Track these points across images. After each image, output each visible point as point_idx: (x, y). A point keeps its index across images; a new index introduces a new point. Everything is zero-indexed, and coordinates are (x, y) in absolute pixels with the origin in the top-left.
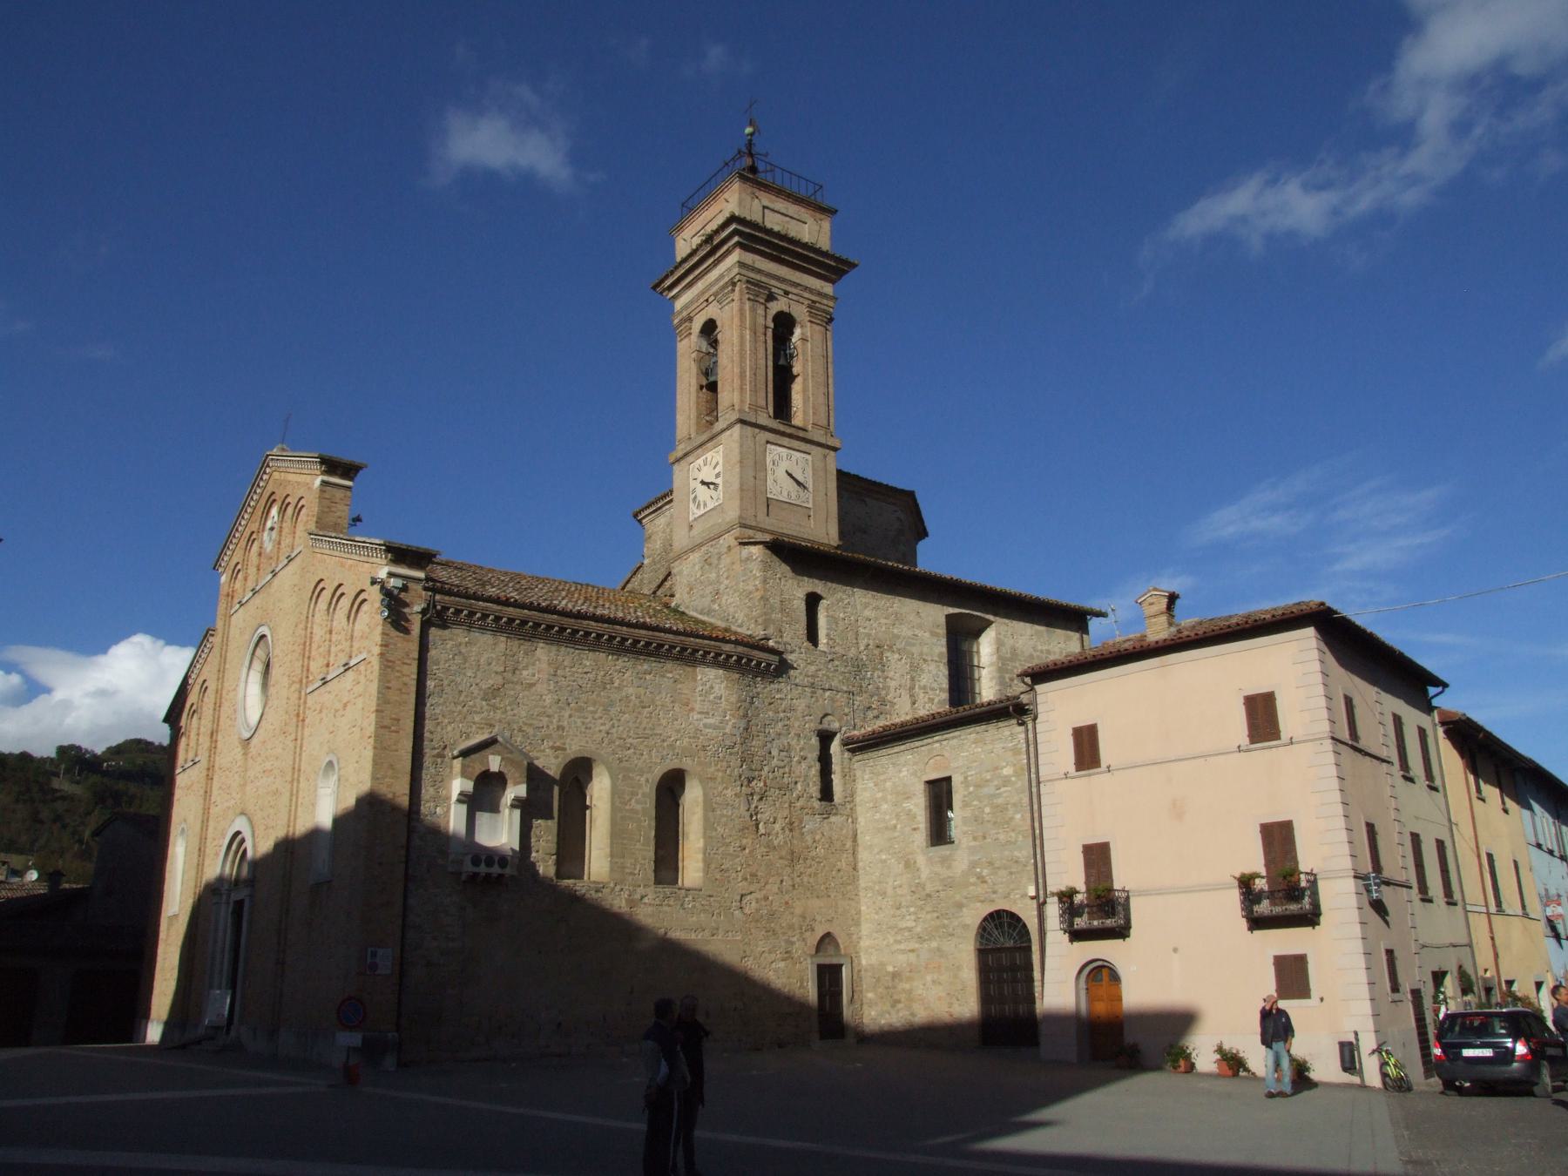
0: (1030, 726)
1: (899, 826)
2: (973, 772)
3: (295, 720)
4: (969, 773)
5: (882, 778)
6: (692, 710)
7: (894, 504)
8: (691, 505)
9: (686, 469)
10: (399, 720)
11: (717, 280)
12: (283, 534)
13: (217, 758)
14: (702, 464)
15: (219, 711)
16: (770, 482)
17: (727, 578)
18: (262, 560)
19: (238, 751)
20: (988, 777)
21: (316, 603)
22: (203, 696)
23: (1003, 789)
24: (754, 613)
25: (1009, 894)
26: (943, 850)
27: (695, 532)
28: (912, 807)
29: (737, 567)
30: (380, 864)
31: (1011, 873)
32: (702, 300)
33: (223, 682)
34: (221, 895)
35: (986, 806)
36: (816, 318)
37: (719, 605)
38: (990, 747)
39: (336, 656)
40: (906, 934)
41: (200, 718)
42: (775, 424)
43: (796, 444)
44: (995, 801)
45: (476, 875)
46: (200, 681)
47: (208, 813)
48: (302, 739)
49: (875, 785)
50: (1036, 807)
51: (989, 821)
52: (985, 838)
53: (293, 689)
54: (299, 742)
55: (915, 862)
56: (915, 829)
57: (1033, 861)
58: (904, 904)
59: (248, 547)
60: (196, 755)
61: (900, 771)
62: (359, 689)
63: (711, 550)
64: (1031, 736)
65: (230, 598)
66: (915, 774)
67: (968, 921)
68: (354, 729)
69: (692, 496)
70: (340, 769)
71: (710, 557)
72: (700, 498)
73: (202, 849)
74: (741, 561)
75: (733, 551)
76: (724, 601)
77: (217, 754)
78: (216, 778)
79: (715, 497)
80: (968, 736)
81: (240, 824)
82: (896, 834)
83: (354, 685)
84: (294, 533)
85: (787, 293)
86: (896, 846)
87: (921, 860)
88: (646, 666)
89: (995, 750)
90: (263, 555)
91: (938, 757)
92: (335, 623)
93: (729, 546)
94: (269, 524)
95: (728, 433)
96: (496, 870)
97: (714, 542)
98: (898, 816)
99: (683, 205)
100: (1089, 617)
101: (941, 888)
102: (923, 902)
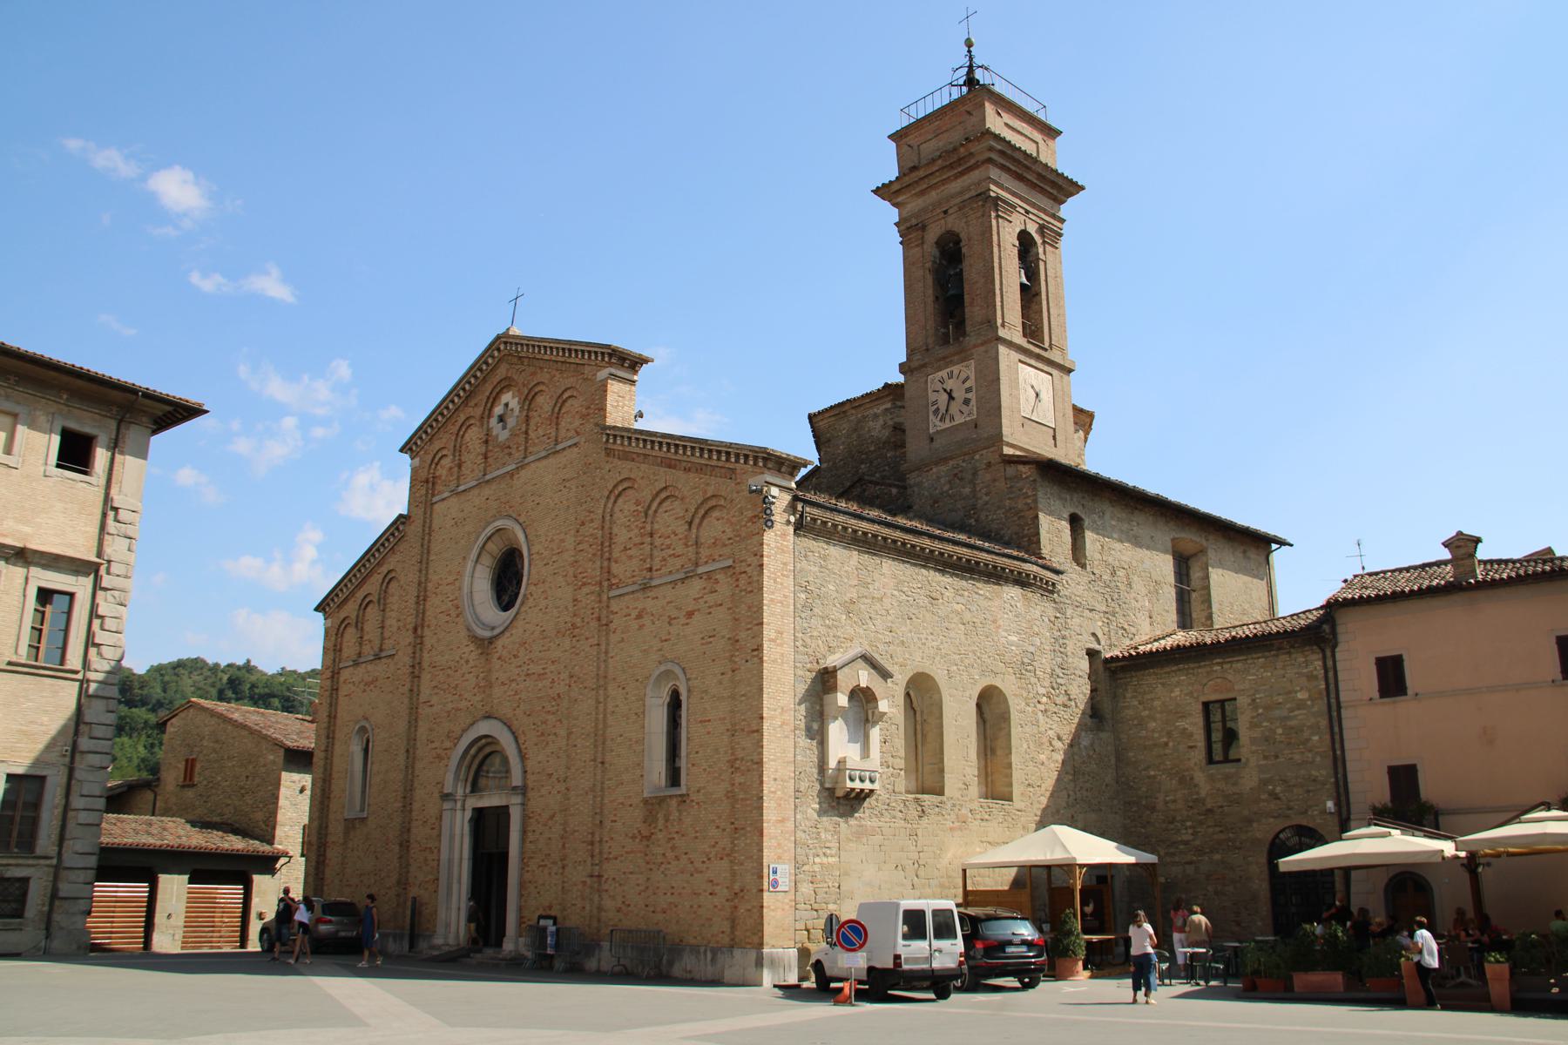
0: (1328, 653)
1: (1171, 744)
2: (1262, 695)
3: (594, 624)
4: (1257, 696)
5: (1149, 697)
6: (999, 627)
8: (931, 417)
9: (923, 380)
10: (782, 634)
12: (532, 423)
13: (426, 655)
14: (945, 377)
15: (424, 605)
16: (1022, 401)
18: (490, 448)
19: (470, 652)
20: (1280, 700)
21: (615, 502)
22: (387, 587)
23: (1296, 713)
25: (1306, 810)
26: (1229, 769)
27: (936, 444)
28: (1186, 726)
29: (1001, 485)
30: (775, 780)
31: (1308, 791)
33: (427, 574)
34: (455, 801)
35: (1277, 727)
36: (1050, 239)
38: (1282, 672)
39: (664, 559)
40: (1182, 847)
41: (383, 610)
44: (1289, 723)
45: (853, 790)
46: (384, 569)
47: (417, 713)
48: (608, 644)
49: (1140, 704)
50: (1336, 729)
51: (1282, 742)
52: (1277, 757)
53: (585, 590)
54: (603, 647)
55: (1192, 779)
56: (1191, 747)
57: (1333, 780)
58: (1179, 818)
59: (461, 433)
60: (381, 650)
61: (1172, 691)
62: (711, 598)
64: (1330, 663)
65: (430, 485)
66: (1191, 694)
67: (1258, 835)
68: (711, 639)
70: (688, 680)
73: (411, 750)
74: (1006, 479)
77: (425, 652)
78: (426, 677)
79: (966, 412)
80: (1256, 661)
81: (484, 728)
82: (1167, 751)
83: (705, 594)
84: (557, 424)
85: (1027, 212)
86: (1168, 763)
87: (1200, 777)
89: (1286, 675)
90: (490, 443)
91: (1219, 680)
92: (656, 526)
93: (990, 463)
94: (498, 410)
96: (867, 786)
98: (1169, 734)
100: (1274, 546)
101: (1225, 804)
102: (1203, 817)
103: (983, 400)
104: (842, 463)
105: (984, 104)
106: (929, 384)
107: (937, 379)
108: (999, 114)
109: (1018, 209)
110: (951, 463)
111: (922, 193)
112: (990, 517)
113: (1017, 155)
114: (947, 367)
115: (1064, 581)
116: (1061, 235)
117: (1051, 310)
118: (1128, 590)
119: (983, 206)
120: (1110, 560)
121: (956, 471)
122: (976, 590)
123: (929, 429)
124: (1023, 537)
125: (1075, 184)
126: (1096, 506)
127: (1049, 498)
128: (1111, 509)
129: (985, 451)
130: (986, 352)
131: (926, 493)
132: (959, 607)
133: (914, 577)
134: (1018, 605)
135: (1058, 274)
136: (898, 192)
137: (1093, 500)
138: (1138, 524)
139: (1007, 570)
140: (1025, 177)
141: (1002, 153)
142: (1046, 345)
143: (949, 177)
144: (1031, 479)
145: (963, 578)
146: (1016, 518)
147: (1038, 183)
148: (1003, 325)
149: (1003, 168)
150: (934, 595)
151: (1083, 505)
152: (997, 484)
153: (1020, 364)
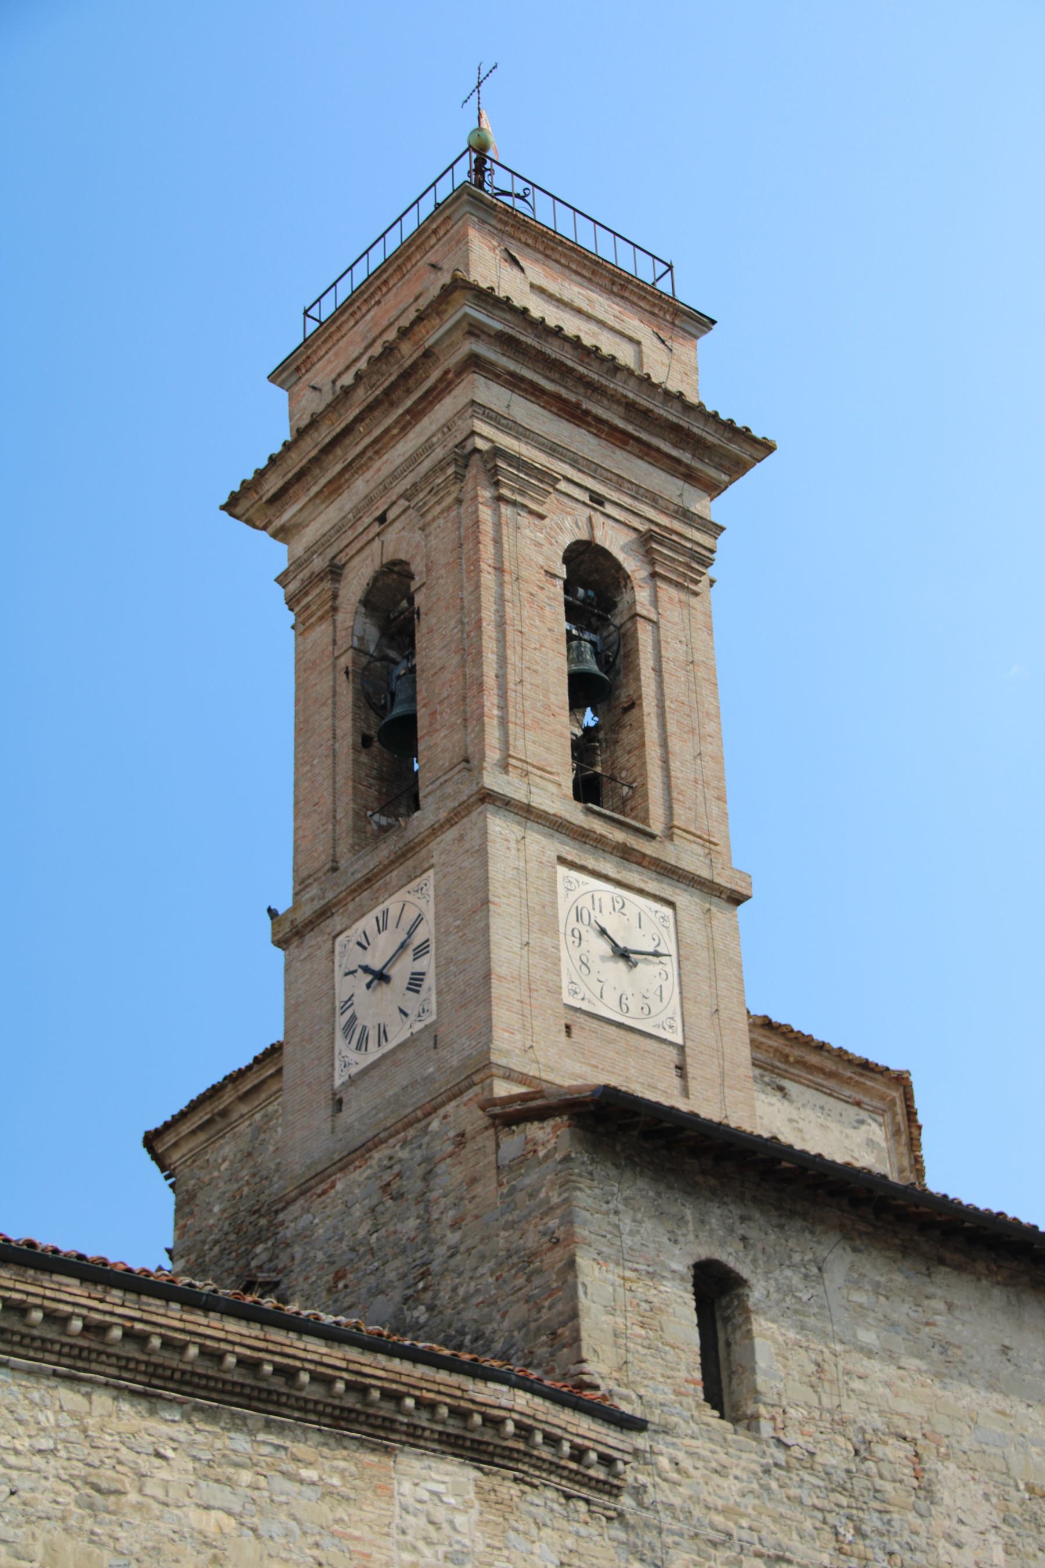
7: (858, 1104)
11: (413, 460)
17: (455, 1226)
24: (545, 1314)
27: (349, 1115)
32: (367, 520)
37: (431, 1308)
42: (574, 813)
43: (634, 876)
63: (404, 1154)
69: (341, 1021)
71: (399, 1175)
72: (368, 1019)
75: (471, 1146)
76: (445, 1295)
79: (412, 1009)
85: (598, 500)
88: (241, 1442)
95: (451, 834)
97: (411, 1132)
99: (306, 313)
103: (453, 968)
104: (216, 1249)
105: (466, 235)
106: (337, 959)
107: (354, 940)
108: (515, 262)
109: (563, 486)
110: (376, 1155)
111: (335, 488)
112: (461, 1291)
113: (553, 349)
114: (376, 902)
115: (664, 1462)
116: (707, 563)
117: (674, 744)
118: (923, 1505)
119: (459, 477)
120: (851, 1408)
121: (387, 1177)
122: (290, 1467)
123: (331, 1076)
124: (538, 1332)
125: (744, 435)
126: (791, 1243)
127: (616, 1212)
128: (849, 1257)
129: (453, 1104)
130: (461, 838)
131: (320, 1256)
132: (210, 1522)
133: (25, 1415)
134: (459, 1519)
135: (698, 657)
136: (279, 497)
137: (781, 1227)
138: (950, 1307)
139: (410, 1402)
140: (587, 413)
141: (507, 342)
142: (657, 826)
143: (387, 431)
144: (558, 1157)
145: (239, 1425)
146: (521, 1281)
147: (630, 428)
148: (504, 766)
149: (515, 383)
150: (106, 1477)
151: (744, 1239)
152: (478, 1189)
153: (562, 871)
